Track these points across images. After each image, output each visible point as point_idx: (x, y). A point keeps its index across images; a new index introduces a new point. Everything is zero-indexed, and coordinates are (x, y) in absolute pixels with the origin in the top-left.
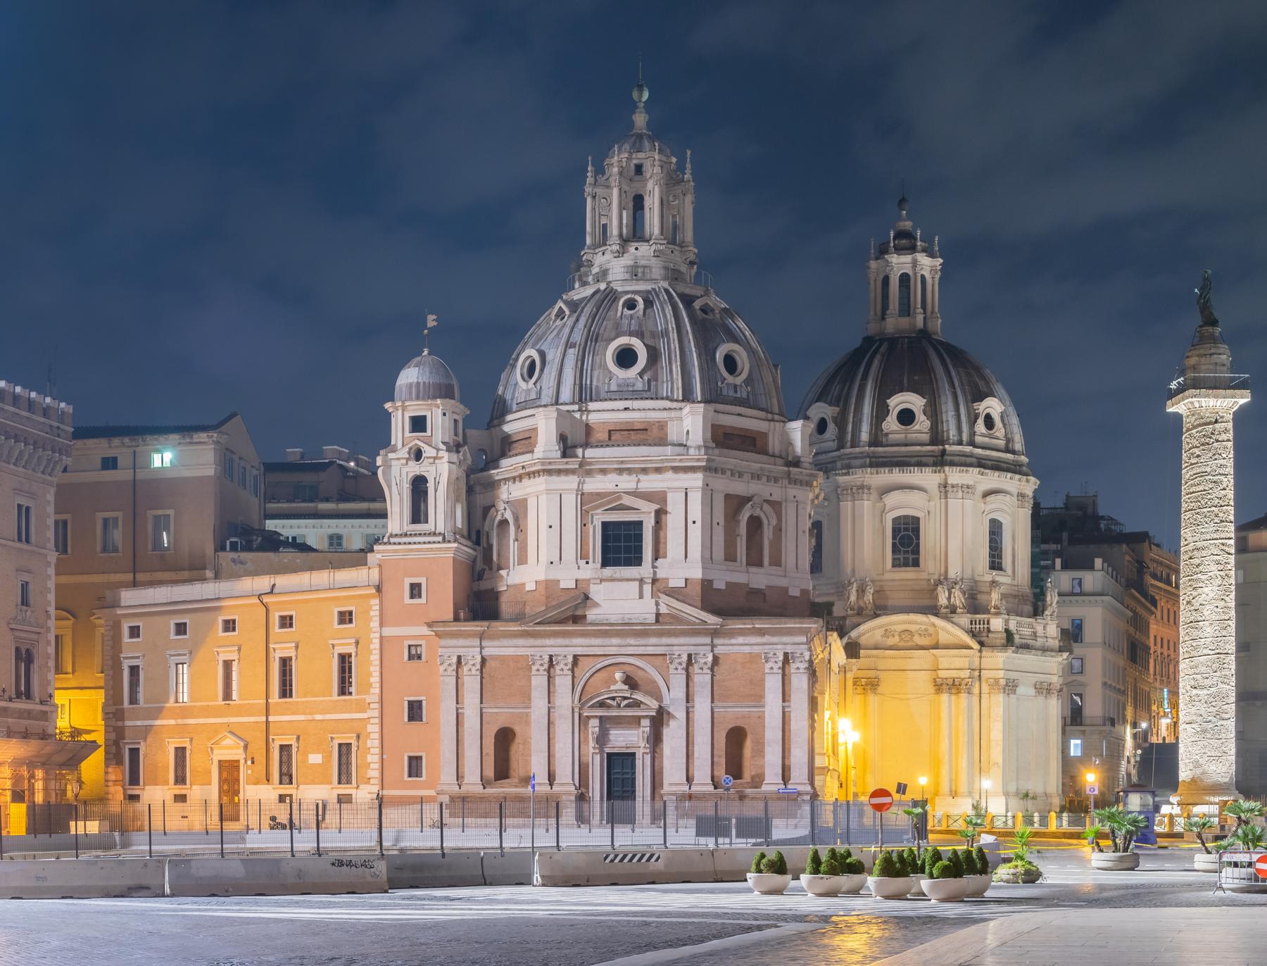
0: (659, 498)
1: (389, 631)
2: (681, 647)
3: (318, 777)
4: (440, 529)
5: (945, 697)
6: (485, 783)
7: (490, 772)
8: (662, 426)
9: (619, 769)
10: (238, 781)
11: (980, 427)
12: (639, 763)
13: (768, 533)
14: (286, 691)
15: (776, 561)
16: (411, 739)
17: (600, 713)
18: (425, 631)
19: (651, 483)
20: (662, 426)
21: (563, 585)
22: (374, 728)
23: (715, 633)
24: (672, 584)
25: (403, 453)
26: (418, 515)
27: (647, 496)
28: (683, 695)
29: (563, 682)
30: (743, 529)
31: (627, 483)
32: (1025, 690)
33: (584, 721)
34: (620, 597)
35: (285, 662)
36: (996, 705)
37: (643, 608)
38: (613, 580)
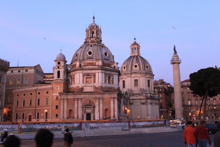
1: (53, 95)
2: (98, 96)
3: (42, 118)
4: (62, 79)
5: (142, 105)
6: (67, 118)
7: (68, 117)
8: (95, 63)
9: (88, 116)
10: (31, 118)
11: (146, 67)
12: (91, 115)
13: (111, 79)
14: (39, 104)
15: (113, 83)
16: (57, 112)
17: (85, 106)
18: (58, 94)
20: (95, 63)
21: (80, 87)
22: (51, 110)
23: (103, 94)
24: (96, 87)
25: (56, 68)
26: (59, 76)
27: (93, 73)
28: (98, 104)
29: (80, 102)
30: (107, 79)
31: (89, 72)
32: (154, 104)
33: (83, 108)
35: (39, 100)
36: (149, 106)
37: (92, 90)
38: (87, 86)
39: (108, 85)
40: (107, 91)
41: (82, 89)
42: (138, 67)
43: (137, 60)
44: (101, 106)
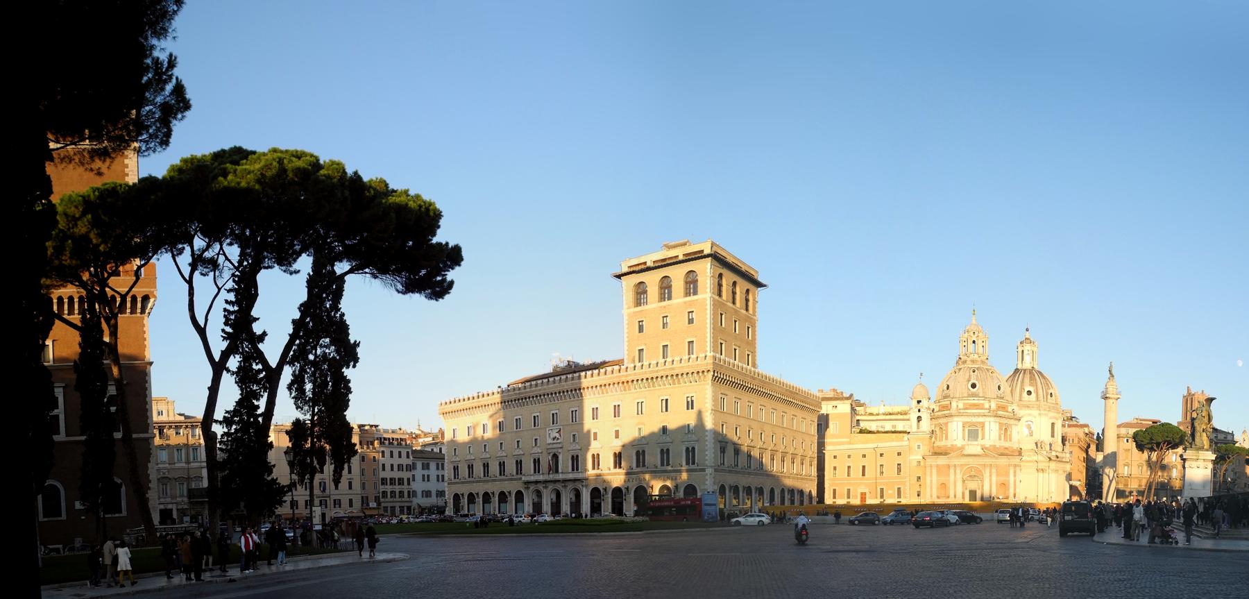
0: (983, 425)
2: (987, 461)
3: (891, 496)
19: (981, 419)
34: (973, 448)
37: (978, 450)
39: (1007, 444)
40: (1002, 455)
41: (963, 448)
42: (1033, 395)
43: (1032, 379)
44: (994, 478)
